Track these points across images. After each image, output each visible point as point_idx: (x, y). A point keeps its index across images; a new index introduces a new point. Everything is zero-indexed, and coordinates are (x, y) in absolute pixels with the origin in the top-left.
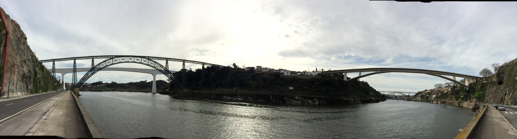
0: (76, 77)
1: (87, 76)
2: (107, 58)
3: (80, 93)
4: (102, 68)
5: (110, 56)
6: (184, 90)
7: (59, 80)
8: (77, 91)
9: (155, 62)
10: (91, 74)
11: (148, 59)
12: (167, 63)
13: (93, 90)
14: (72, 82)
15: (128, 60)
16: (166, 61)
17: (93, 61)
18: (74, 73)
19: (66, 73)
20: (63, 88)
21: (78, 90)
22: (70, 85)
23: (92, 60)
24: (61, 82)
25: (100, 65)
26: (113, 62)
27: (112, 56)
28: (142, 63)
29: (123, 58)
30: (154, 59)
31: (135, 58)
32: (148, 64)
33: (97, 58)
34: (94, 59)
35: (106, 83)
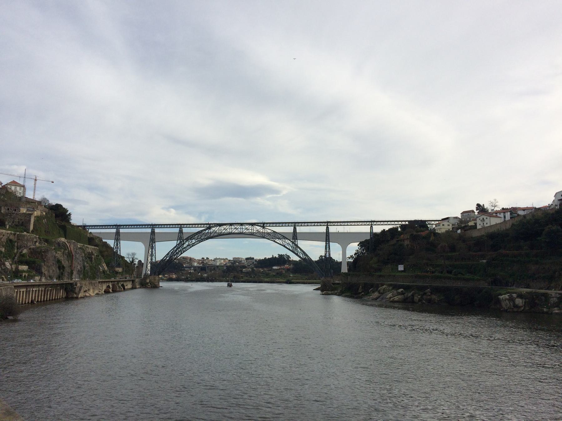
2: (202, 227)
11: (263, 227)
29: (225, 227)
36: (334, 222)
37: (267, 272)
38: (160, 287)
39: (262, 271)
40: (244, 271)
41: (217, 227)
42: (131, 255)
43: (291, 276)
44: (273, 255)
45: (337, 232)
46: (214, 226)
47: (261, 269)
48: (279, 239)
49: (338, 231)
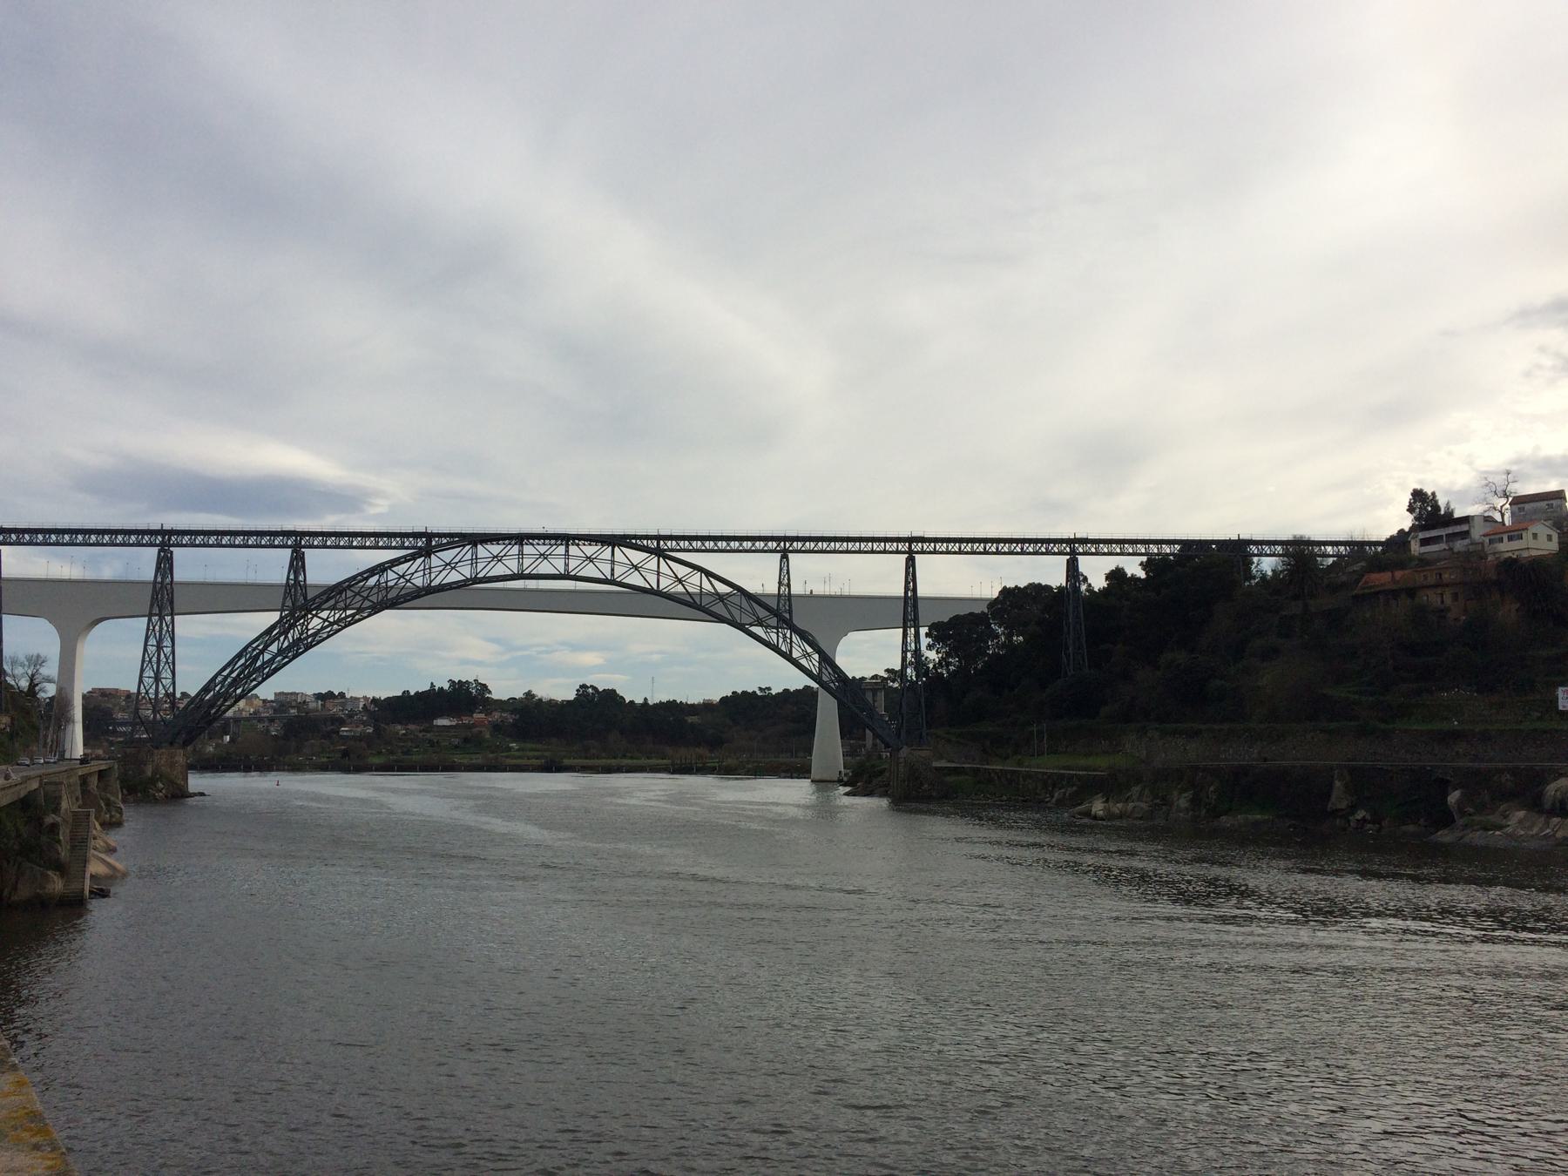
0: (166, 674)
2: (395, 548)
8: (172, 765)
11: (659, 553)
27: (429, 536)
29: (495, 549)
31: (573, 550)
35: (529, 695)
36: (936, 540)
38: (195, 795)
39: (404, 732)
40: (345, 734)
41: (464, 546)
42: (22, 665)
43: (512, 747)
44: (432, 683)
45: (808, 593)
46: (448, 543)
47: (399, 727)
48: (721, 598)
49: (811, 592)
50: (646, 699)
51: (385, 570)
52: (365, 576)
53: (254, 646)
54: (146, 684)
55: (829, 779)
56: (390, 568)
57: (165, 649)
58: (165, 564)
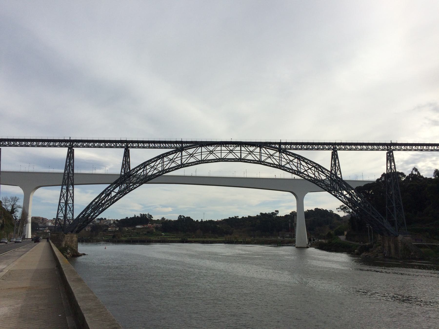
0: (70, 202)
1: (105, 197)
2: (166, 148)
3: (82, 248)
4: (152, 175)
5: (176, 142)
6: (400, 237)
7: (10, 208)
8: (72, 241)
9: (299, 158)
10: (118, 193)
11: (280, 150)
12: (335, 157)
13: (123, 239)
14: (58, 214)
15: (223, 155)
16: (330, 152)
17: (127, 155)
18: (65, 187)
19: (37, 188)
20: (22, 234)
21: (75, 239)
22: (50, 224)
23: (125, 153)
24: (18, 214)
25: (148, 167)
26: (183, 160)
27: (182, 142)
28: (263, 162)
29: (211, 148)
30: (296, 149)
31: (243, 149)
32: (279, 165)
33: (138, 147)
34: (131, 150)
37: (132, 230)
40: (110, 230)
44: (135, 215)
47: (126, 228)
49: (294, 178)
50: (202, 220)
51: (163, 157)
52: (155, 159)
53: (109, 189)
54: (62, 206)
55: (303, 247)
56: (167, 156)
57: (70, 191)
58: (71, 155)
